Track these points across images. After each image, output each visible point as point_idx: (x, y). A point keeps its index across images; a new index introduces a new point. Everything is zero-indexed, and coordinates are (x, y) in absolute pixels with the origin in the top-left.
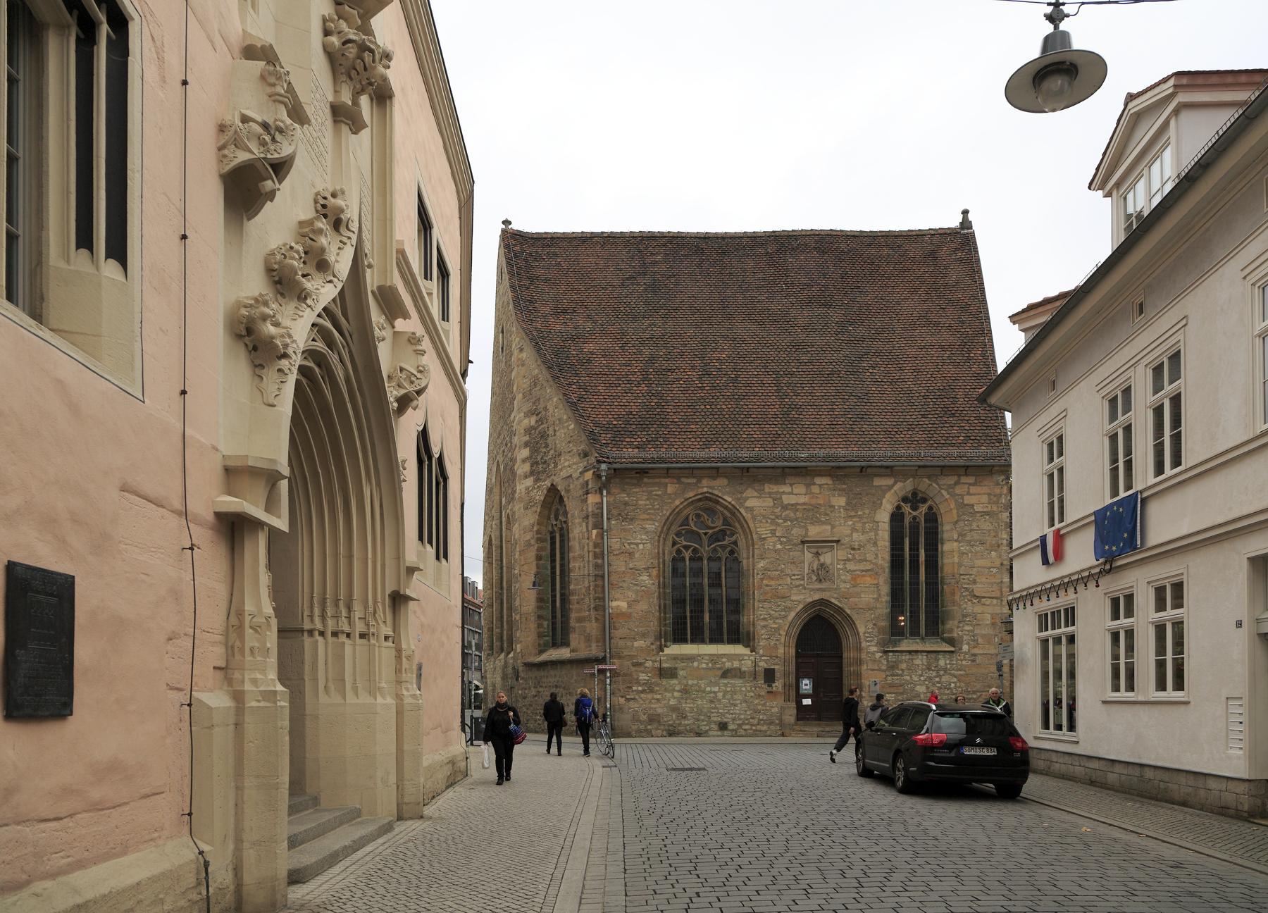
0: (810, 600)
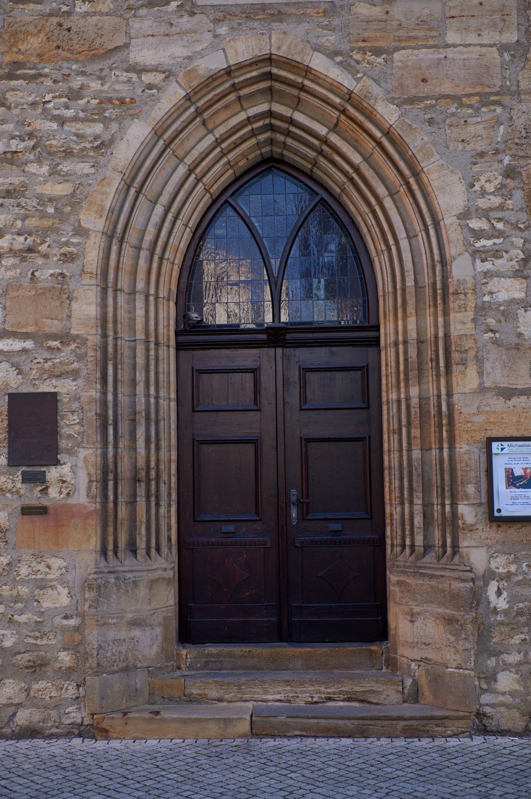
0: (216, 62)
